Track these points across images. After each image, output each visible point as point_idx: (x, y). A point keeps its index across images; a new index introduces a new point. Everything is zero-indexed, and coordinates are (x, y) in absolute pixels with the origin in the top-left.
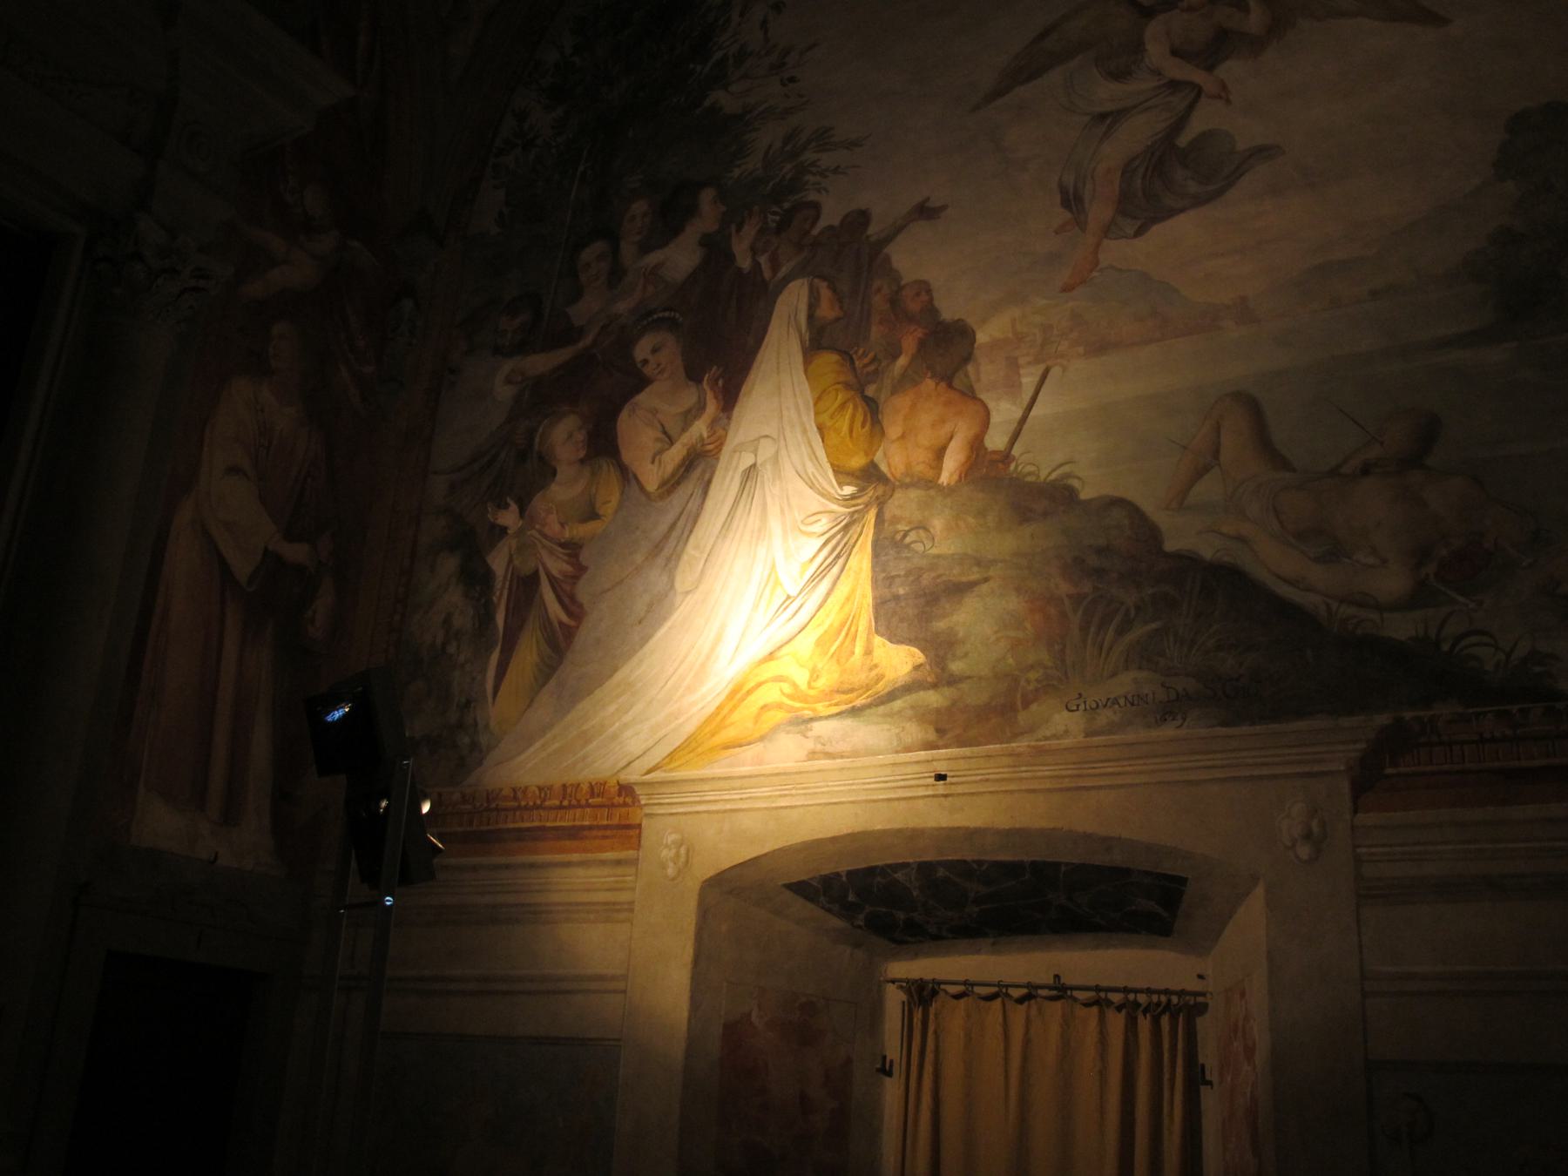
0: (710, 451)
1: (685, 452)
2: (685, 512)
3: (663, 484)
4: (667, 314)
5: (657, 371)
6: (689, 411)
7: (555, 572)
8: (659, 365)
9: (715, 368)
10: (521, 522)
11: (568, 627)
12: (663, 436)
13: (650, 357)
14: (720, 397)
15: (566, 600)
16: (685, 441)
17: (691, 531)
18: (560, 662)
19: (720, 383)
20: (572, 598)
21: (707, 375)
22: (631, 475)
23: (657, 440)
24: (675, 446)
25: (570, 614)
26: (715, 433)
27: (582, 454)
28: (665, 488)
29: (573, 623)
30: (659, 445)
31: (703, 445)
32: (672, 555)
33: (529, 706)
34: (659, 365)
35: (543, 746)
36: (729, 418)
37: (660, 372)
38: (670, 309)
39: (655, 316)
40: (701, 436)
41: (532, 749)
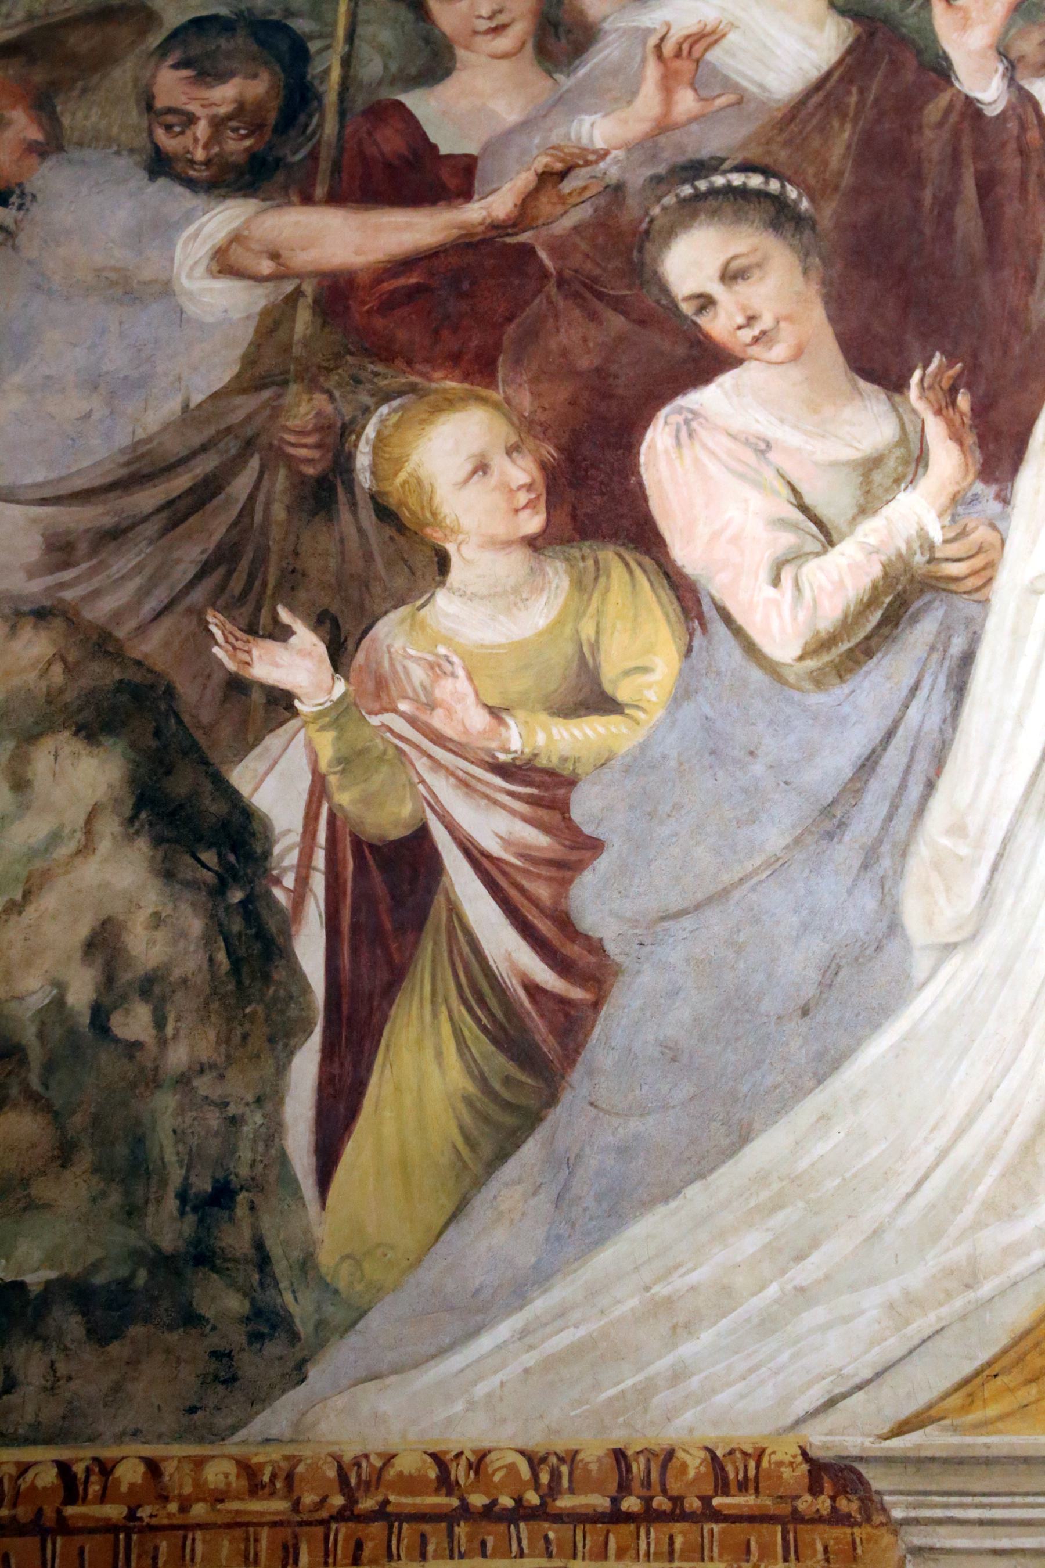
0: (956, 579)
1: (876, 571)
2: (900, 732)
3: (821, 645)
4: (755, 181)
5: (746, 335)
6: (872, 464)
7: (494, 847)
8: (751, 320)
9: (937, 359)
10: (340, 687)
11: (563, 1001)
12: (799, 516)
13: (716, 289)
14: (971, 439)
15: (544, 927)
16: (873, 540)
17: (930, 786)
18: (552, 1100)
19: (963, 401)
20: (565, 922)
21: (917, 375)
22: (707, 607)
23: (782, 523)
24: (839, 548)
25: (562, 966)
26: (963, 534)
27: (533, 523)
28: (826, 658)
29: (577, 994)
30: (787, 539)
31: (931, 560)
32: (879, 841)
33: (454, 1217)
34: (751, 320)
35: (524, 1333)
36: (1005, 499)
37: (756, 340)
38: (767, 172)
39: (719, 181)
40: (922, 534)
41: (485, 1342)
